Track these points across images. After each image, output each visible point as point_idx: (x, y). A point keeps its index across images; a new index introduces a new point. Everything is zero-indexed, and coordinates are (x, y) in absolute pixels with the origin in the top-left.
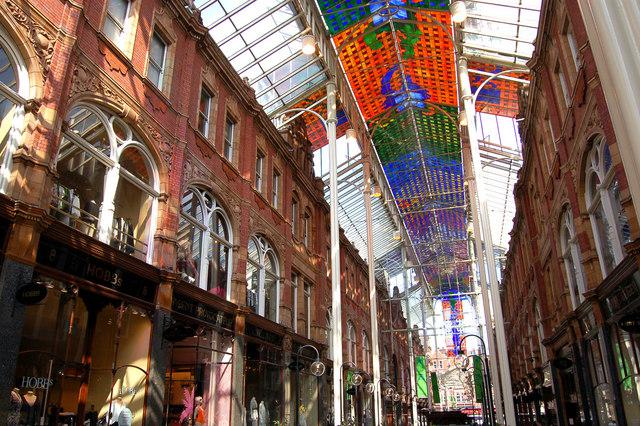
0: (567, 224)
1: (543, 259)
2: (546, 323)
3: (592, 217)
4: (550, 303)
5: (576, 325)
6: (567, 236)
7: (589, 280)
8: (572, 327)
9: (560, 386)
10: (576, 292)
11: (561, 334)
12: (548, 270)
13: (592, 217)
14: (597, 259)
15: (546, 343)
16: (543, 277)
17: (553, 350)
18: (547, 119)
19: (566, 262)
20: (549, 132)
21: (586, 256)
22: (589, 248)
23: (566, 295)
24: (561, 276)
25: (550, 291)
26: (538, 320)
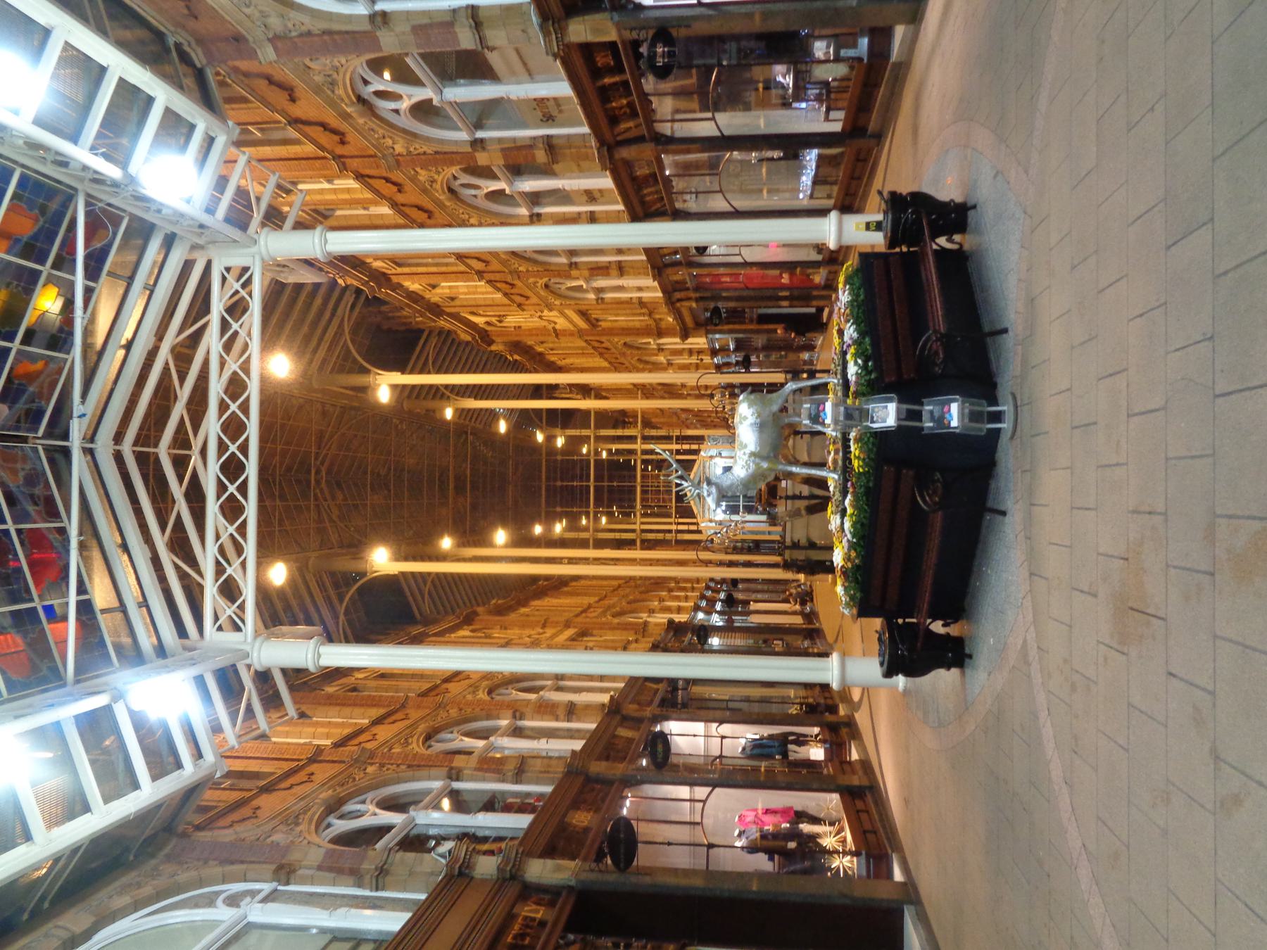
0: (563, 287)
1: (582, 324)
2: (660, 333)
3: (575, 259)
4: (637, 325)
5: (678, 295)
6: (579, 288)
7: (639, 274)
8: (679, 300)
9: (737, 327)
10: (640, 289)
11: (679, 316)
12: (597, 320)
13: (575, 259)
14: (620, 262)
15: (685, 335)
16: (604, 329)
17: (694, 329)
18: (434, 287)
19: (602, 295)
20: (450, 287)
21: (614, 272)
22: (607, 268)
23: (641, 303)
24: (618, 303)
25: (622, 320)
26: (652, 342)
